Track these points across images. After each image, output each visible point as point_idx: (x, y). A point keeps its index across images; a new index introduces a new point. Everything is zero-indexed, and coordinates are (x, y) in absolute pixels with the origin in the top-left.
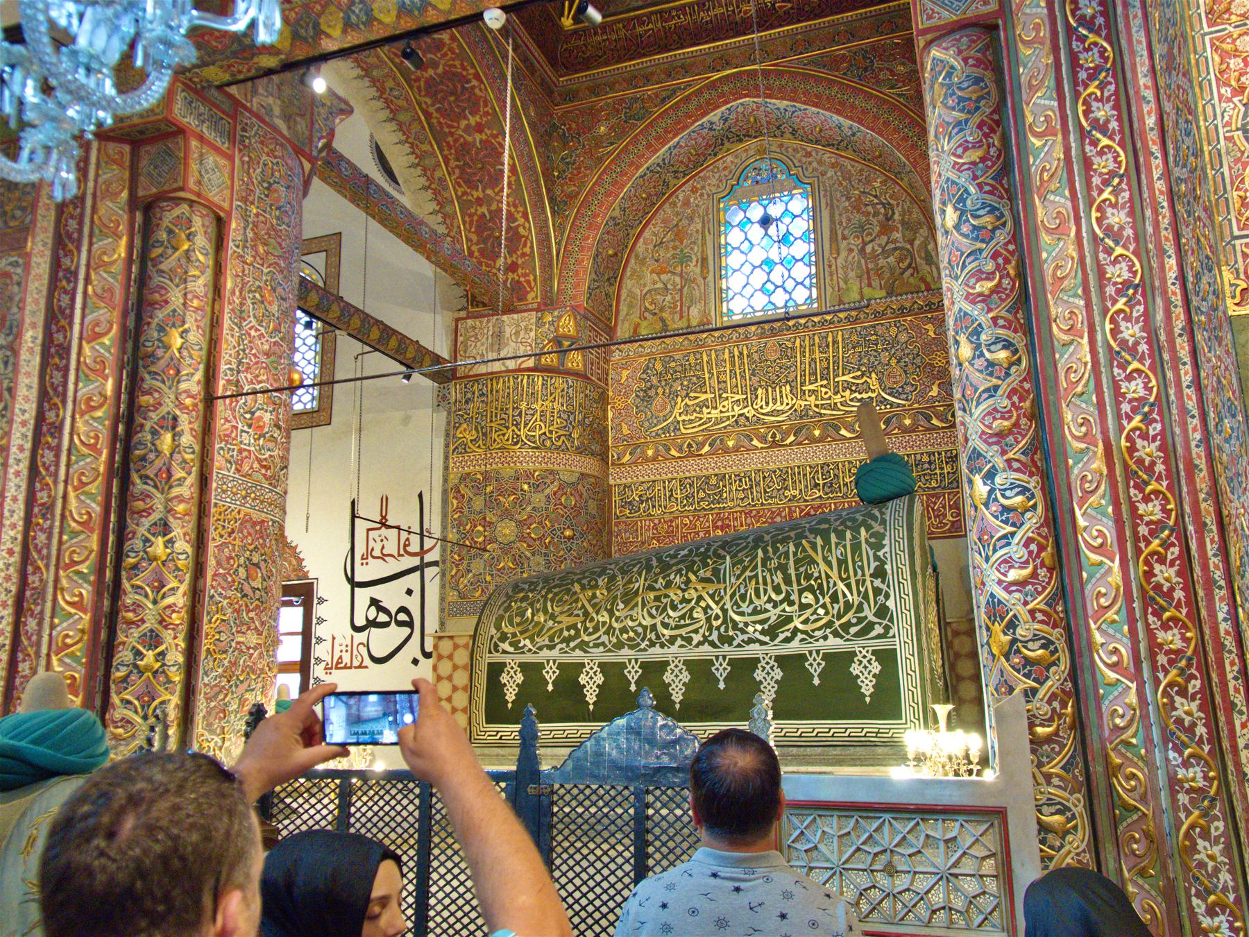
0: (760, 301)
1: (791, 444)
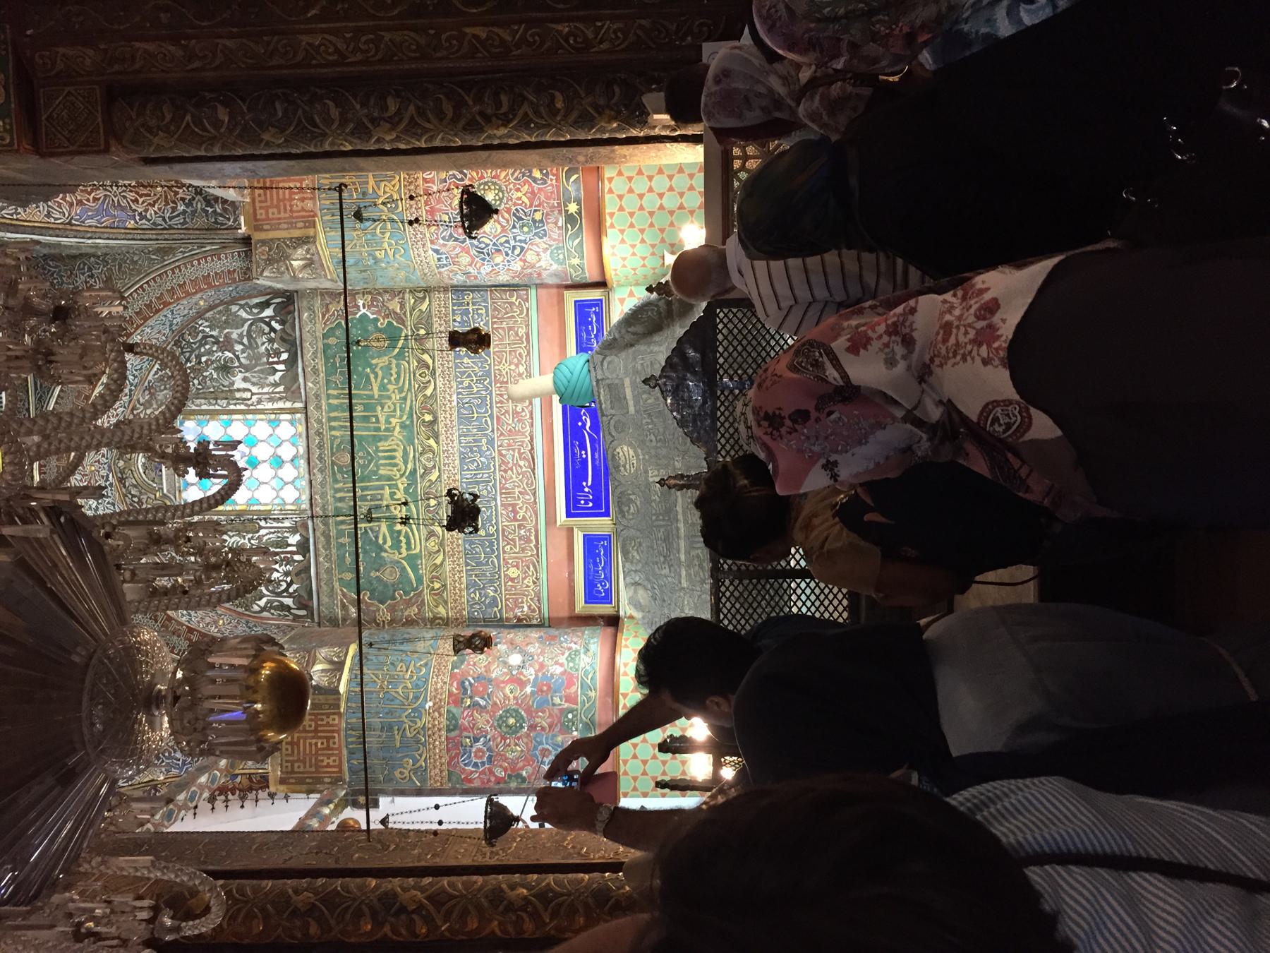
0: (288, 472)
1: (437, 442)
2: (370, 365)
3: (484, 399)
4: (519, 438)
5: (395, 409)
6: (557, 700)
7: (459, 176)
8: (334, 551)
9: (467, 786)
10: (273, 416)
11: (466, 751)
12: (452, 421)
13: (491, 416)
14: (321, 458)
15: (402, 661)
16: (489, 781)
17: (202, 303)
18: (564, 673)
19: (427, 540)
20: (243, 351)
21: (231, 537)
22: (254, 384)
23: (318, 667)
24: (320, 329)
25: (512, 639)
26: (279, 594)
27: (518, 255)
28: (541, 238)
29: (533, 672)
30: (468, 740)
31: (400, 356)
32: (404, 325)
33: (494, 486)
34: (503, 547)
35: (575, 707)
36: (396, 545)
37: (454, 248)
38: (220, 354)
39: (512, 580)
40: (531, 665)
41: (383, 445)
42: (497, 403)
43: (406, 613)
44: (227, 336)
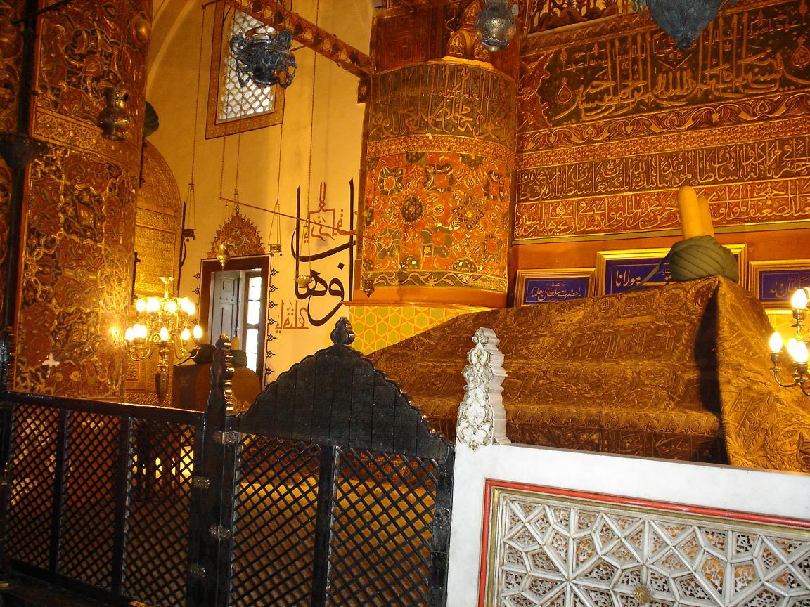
1: (689, 129)
3: (734, 173)
5: (724, 82)
6: (427, 250)
8: (587, 42)
11: (393, 172)
12: (711, 141)
15: (472, 110)
16: (369, 193)
18: (452, 257)
19: (593, 126)
23: (466, 34)
25: (492, 210)
29: (455, 228)
31: (785, 83)
36: (590, 98)
39: (554, 209)
40: (461, 227)
41: (687, 75)
42: (729, 187)
43: (529, 113)
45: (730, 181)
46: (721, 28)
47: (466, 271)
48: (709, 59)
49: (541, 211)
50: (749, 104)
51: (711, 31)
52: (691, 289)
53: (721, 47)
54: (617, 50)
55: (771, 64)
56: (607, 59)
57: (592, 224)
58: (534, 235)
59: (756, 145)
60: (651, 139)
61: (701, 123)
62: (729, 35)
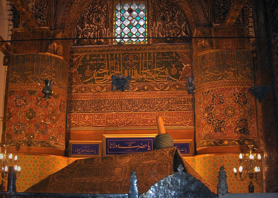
1: (137, 91)
2: (165, 68)
4: (137, 121)
5: (149, 76)
6: (38, 132)
7: (236, 101)
8: (97, 53)
9: (9, 98)
10: (147, 34)
12: (144, 96)
13: (146, 111)
14: (131, 50)
16: (10, 105)
17: (187, 12)
19: (100, 86)
20: (170, 25)
21: (104, 19)
22: (158, 28)
23: (55, 44)
24: (178, 51)
25: (62, 116)
26: (82, 34)
27: (207, 122)
28: (214, 130)
29: (49, 123)
30: (25, 98)
32: (180, 80)
33: (120, 111)
34: (96, 114)
35: (35, 139)
36: (99, 75)
37: (210, 98)
38: (169, 17)
39: (84, 117)
40: (51, 122)
41: (136, 71)
44: (175, 20)
45: (151, 111)
46: (147, 56)
47: (53, 141)
48: (143, 67)
49: (79, 117)
50: (157, 85)
51: (144, 57)
52: (167, 151)
53: (147, 63)
54: (109, 58)
55: (164, 72)
56: (105, 61)
57: (100, 124)
58: (76, 127)
59: (160, 99)
60: (122, 93)
61: (141, 89)
62: (150, 59)
